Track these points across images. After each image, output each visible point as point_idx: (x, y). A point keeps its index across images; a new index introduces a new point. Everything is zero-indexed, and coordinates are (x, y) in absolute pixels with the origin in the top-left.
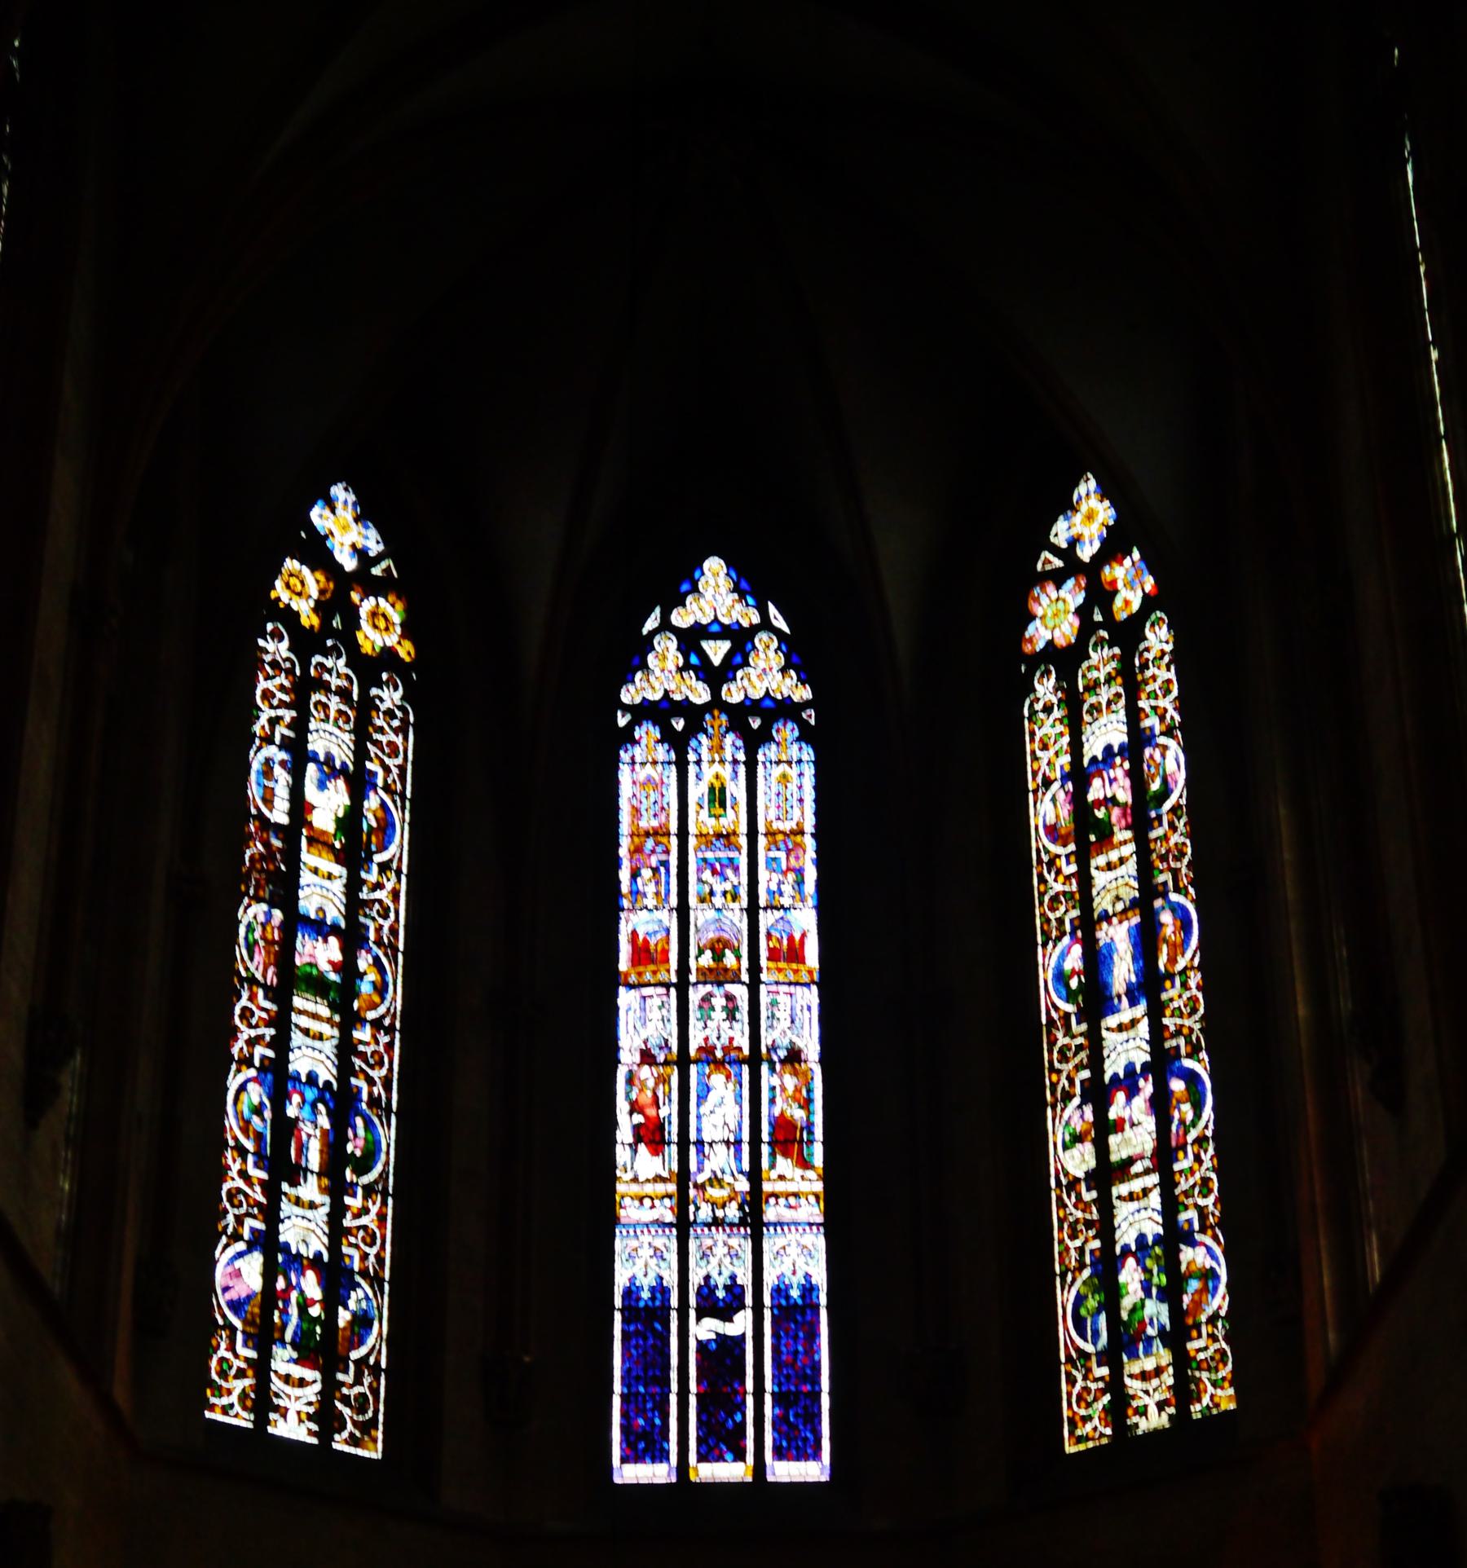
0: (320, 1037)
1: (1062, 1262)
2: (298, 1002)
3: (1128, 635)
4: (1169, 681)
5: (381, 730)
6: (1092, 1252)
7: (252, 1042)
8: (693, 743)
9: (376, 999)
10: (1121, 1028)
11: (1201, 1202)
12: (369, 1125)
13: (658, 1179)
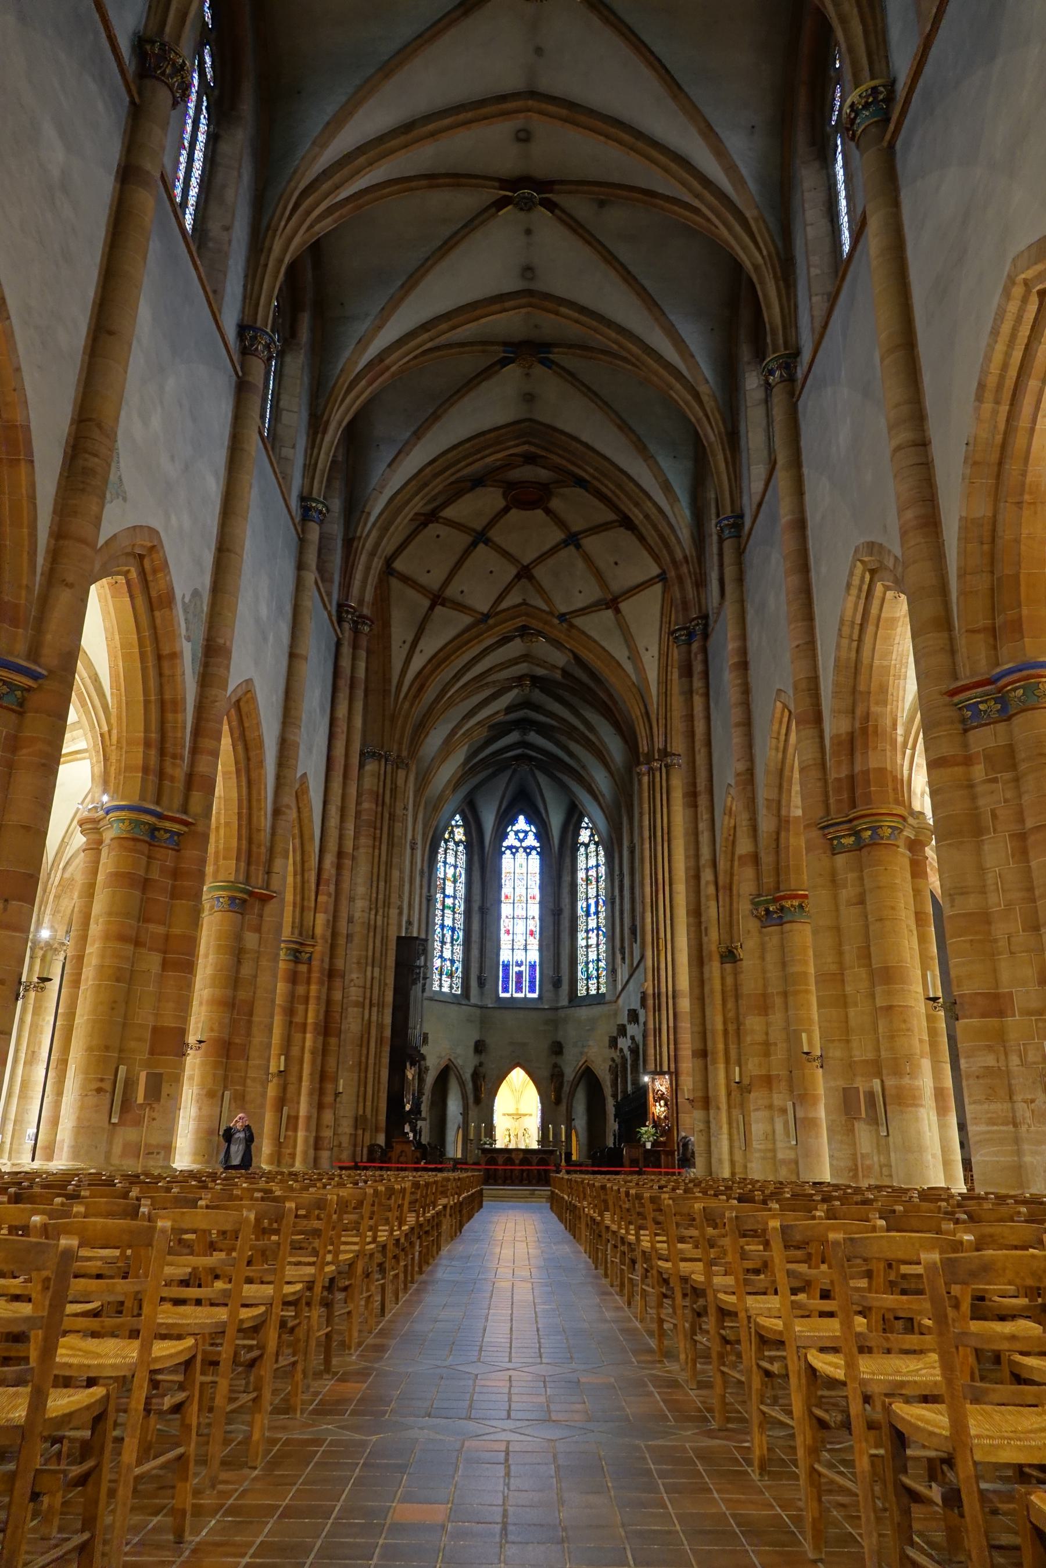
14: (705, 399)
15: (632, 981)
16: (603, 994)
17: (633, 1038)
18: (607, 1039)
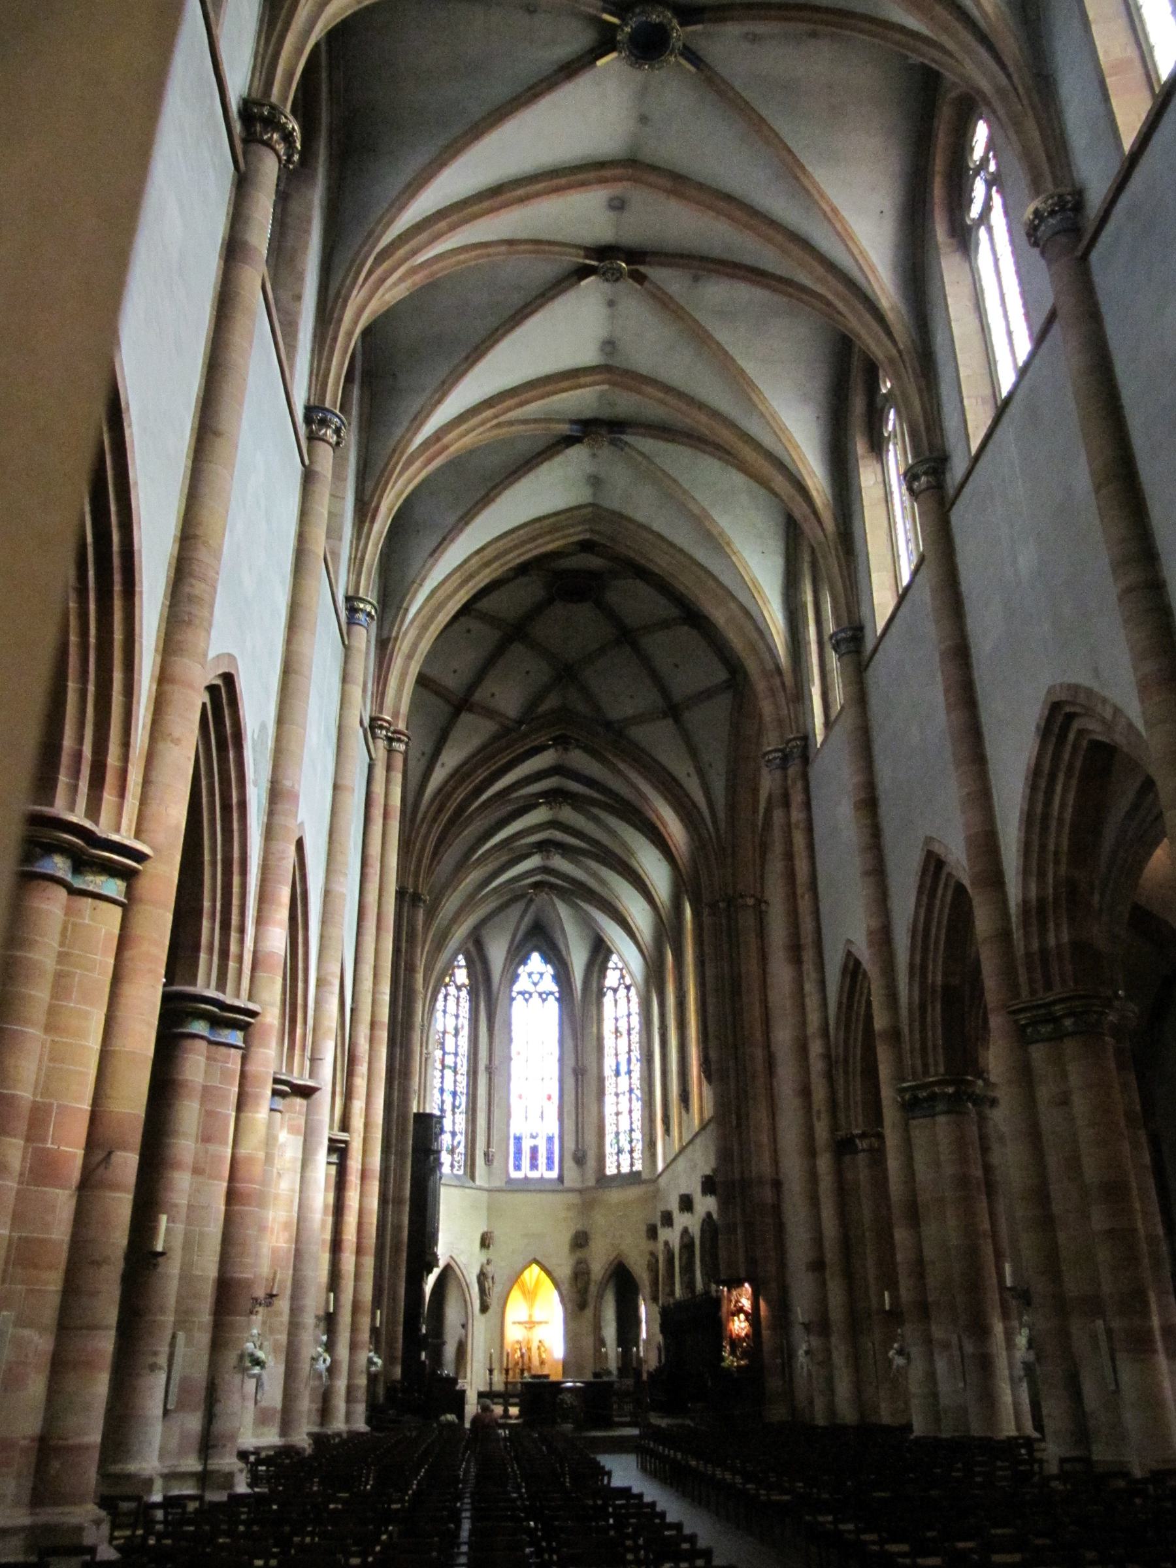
14: (814, 493)
16: (638, 1173)
17: (685, 1231)
18: (643, 1228)
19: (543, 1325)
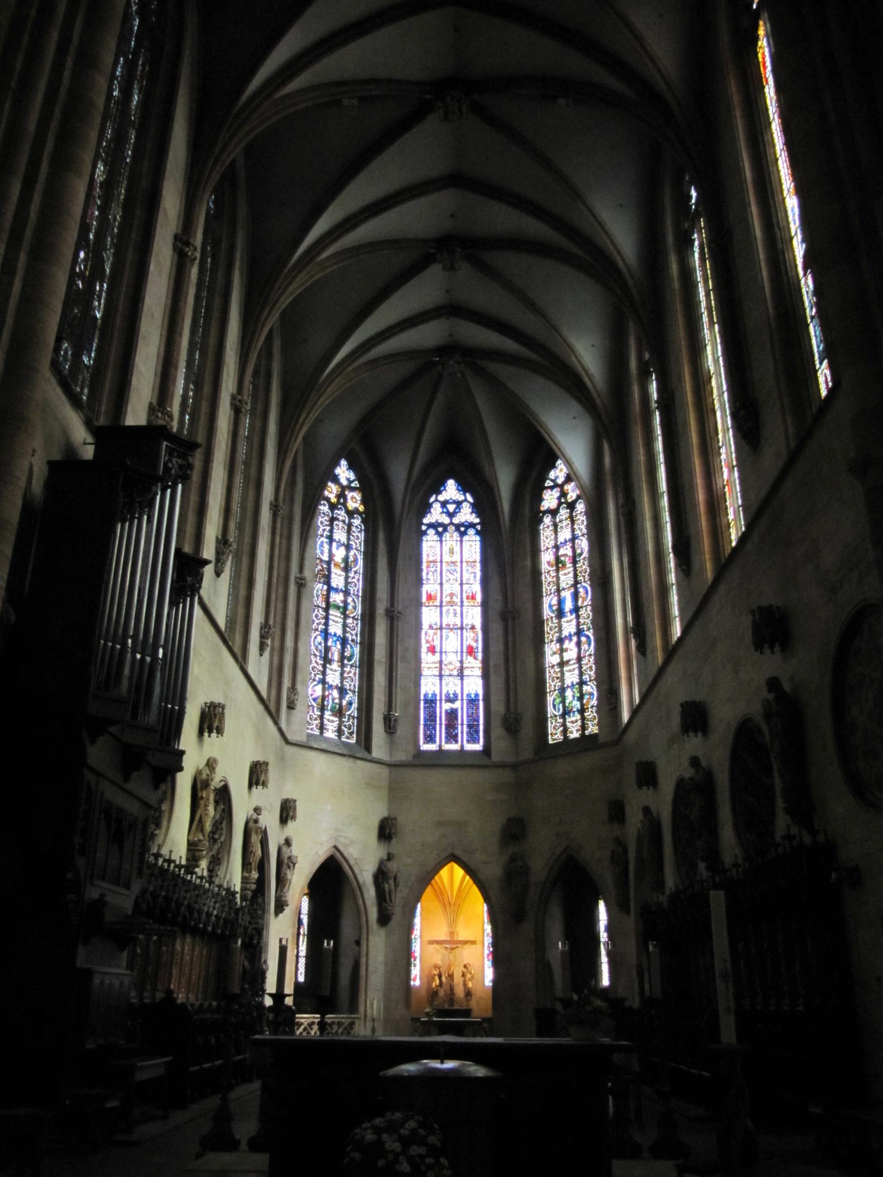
0: (337, 622)
1: (549, 688)
2: (331, 612)
3: (571, 506)
4: (583, 521)
5: (354, 532)
6: (558, 686)
7: (318, 624)
8: (444, 535)
9: (353, 611)
10: (568, 622)
11: (589, 673)
12: (351, 647)
13: (434, 663)
15: (722, 588)
16: (593, 737)
19: (467, 946)
